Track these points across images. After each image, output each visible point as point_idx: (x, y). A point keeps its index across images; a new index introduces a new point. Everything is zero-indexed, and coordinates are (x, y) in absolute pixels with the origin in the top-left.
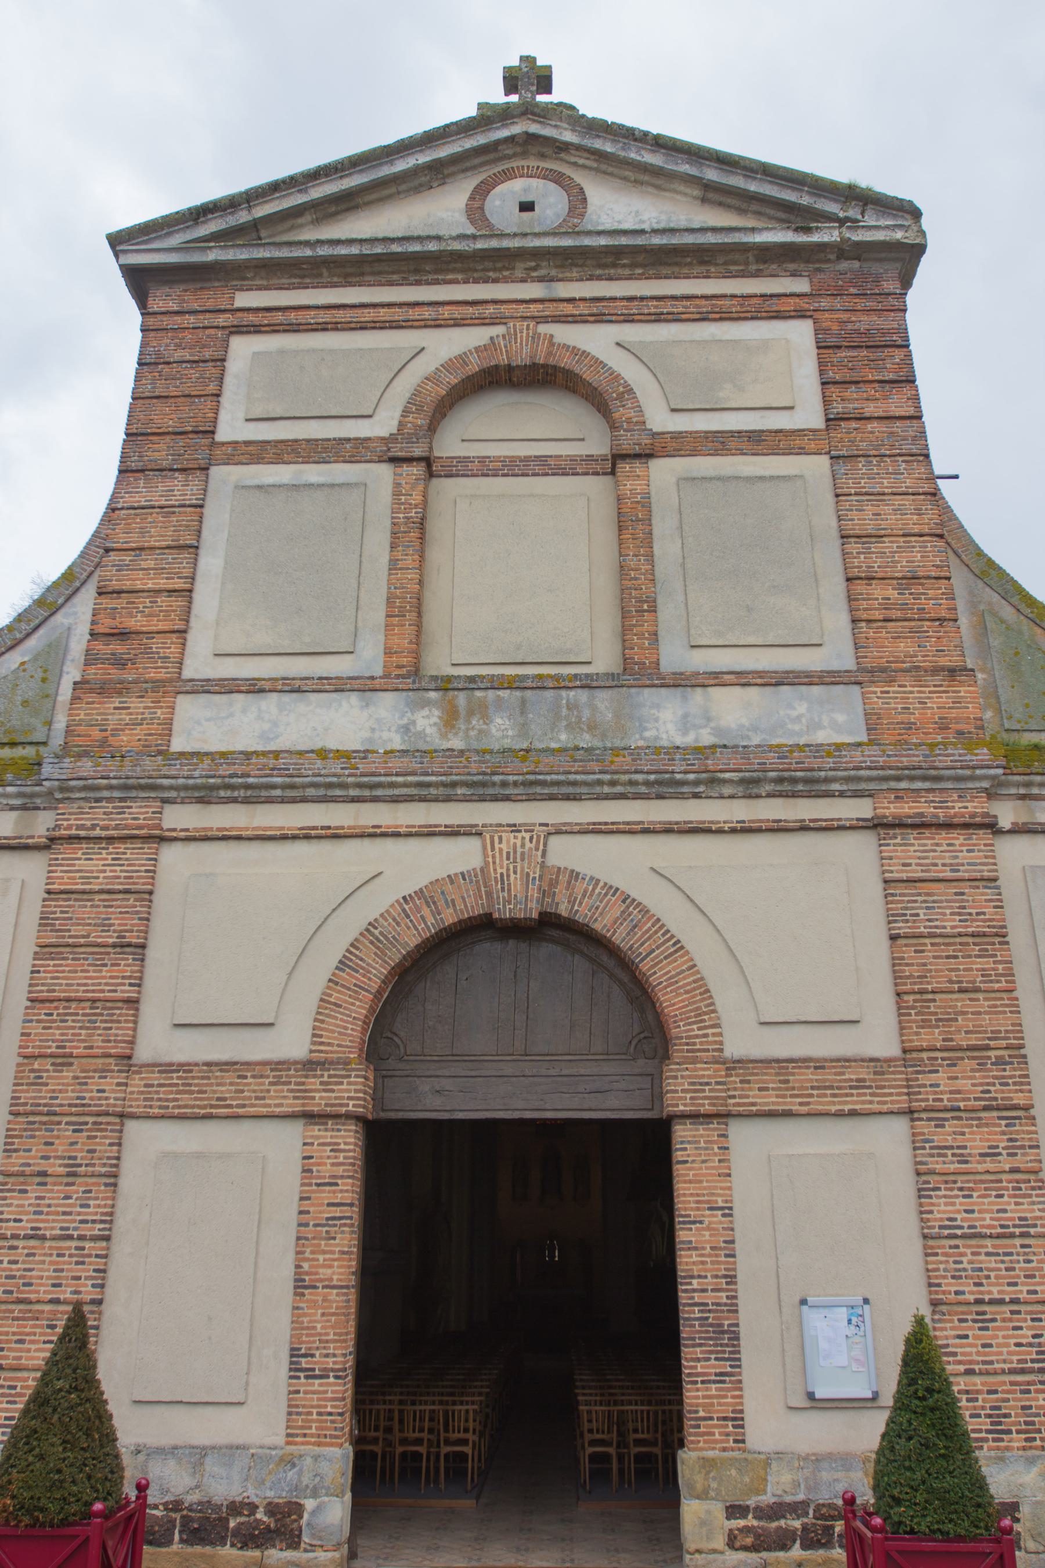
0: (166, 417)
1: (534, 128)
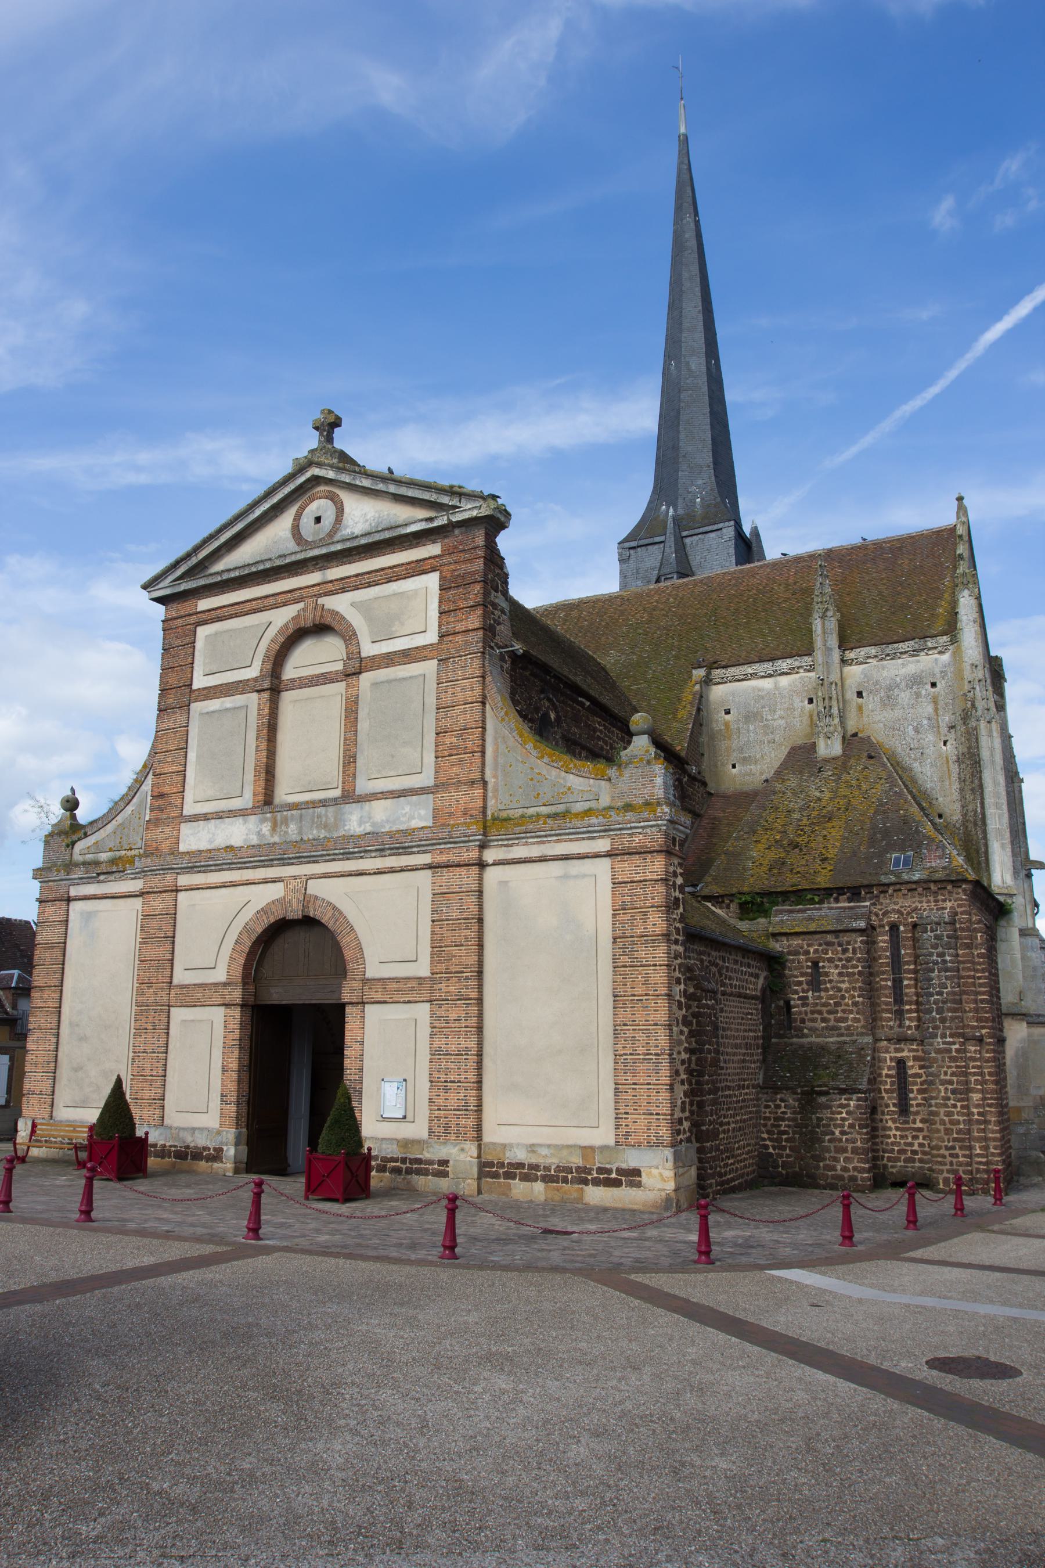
0: (173, 680)
1: (316, 471)
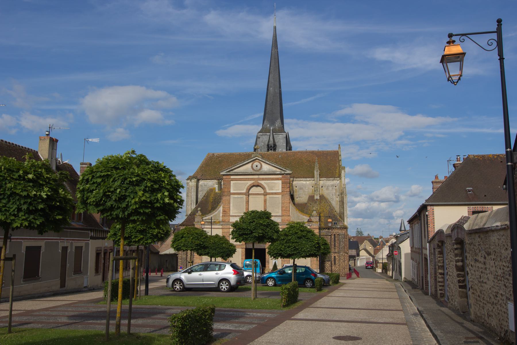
1: (257, 158)
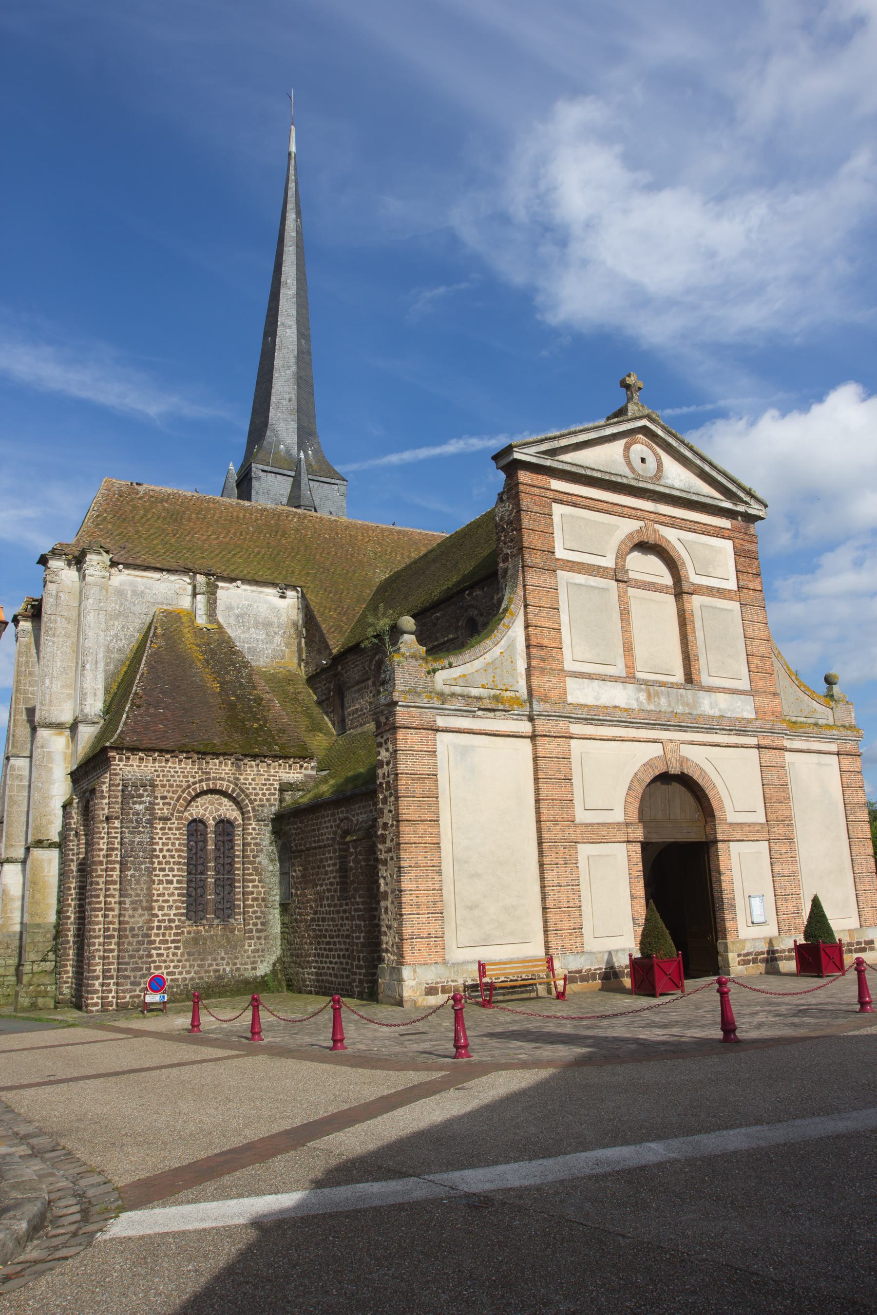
1: (648, 424)
